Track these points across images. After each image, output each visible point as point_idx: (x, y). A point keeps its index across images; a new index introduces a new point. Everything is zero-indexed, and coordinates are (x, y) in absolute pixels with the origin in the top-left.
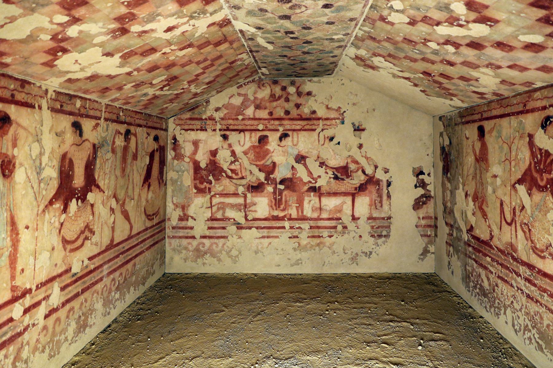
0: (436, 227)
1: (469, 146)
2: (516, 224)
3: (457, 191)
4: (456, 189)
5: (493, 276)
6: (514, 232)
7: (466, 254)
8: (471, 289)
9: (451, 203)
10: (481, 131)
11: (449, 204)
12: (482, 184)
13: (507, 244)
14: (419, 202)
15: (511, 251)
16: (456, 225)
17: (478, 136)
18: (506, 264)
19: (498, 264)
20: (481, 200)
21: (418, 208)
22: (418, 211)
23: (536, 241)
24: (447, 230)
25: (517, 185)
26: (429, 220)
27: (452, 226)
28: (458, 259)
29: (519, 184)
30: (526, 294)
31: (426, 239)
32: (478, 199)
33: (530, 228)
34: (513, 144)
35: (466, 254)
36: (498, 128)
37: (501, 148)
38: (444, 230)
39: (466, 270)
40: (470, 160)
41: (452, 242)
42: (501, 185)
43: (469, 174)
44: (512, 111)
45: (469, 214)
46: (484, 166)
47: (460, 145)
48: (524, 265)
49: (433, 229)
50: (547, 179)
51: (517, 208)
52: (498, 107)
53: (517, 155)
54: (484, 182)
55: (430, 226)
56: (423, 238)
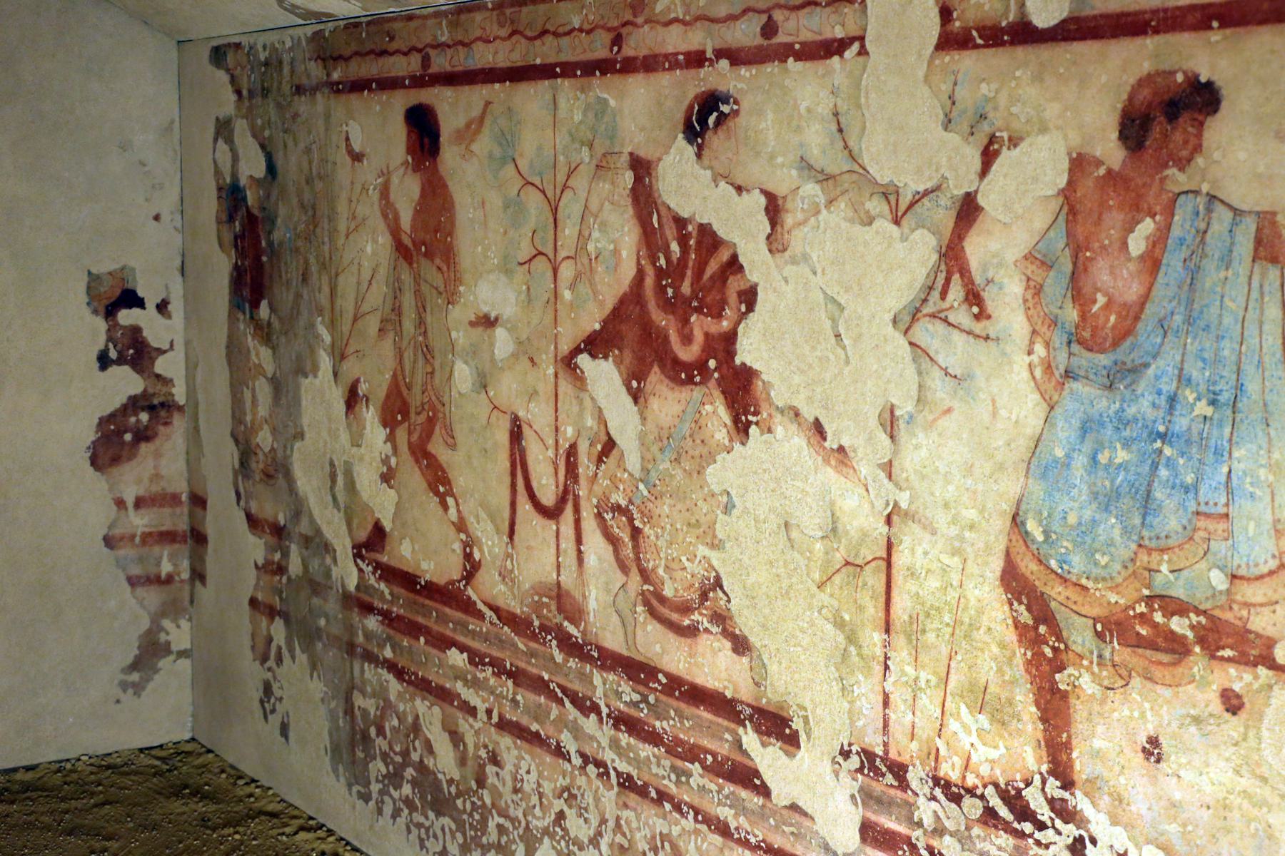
0: (198, 538)
1: (365, 189)
2: (577, 510)
3: (305, 382)
4: (301, 371)
5: (478, 725)
6: (568, 544)
7: (351, 648)
8: (375, 788)
9: (274, 431)
10: (423, 131)
11: (264, 439)
12: (428, 352)
13: (540, 589)
14: (120, 433)
15: (559, 619)
16: (304, 527)
17: (410, 150)
18: (534, 671)
19: (497, 675)
20: (422, 418)
21: (116, 460)
22: (115, 471)
23: (661, 571)
24: (256, 548)
25: (583, 360)
26: (167, 511)
27: (279, 531)
28: (313, 667)
29: (594, 356)
30: (619, 774)
31: (153, 597)
32: (406, 415)
33: (637, 523)
34: (568, 195)
35: (351, 648)
36: (502, 122)
37: (514, 207)
38: (238, 552)
39: (349, 711)
40: (369, 250)
41: (284, 602)
42: (515, 356)
43: (366, 307)
44: (563, 58)
45: (367, 478)
46: (438, 280)
47: (319, 185)
48: (612, 669)
49: (184, 550)
50: (707, 335)
51: (583, 447)
52: (504, 32)
53: (582, 238)
54: (437, 342)
55: (168, 537)
56: (140, 591)
